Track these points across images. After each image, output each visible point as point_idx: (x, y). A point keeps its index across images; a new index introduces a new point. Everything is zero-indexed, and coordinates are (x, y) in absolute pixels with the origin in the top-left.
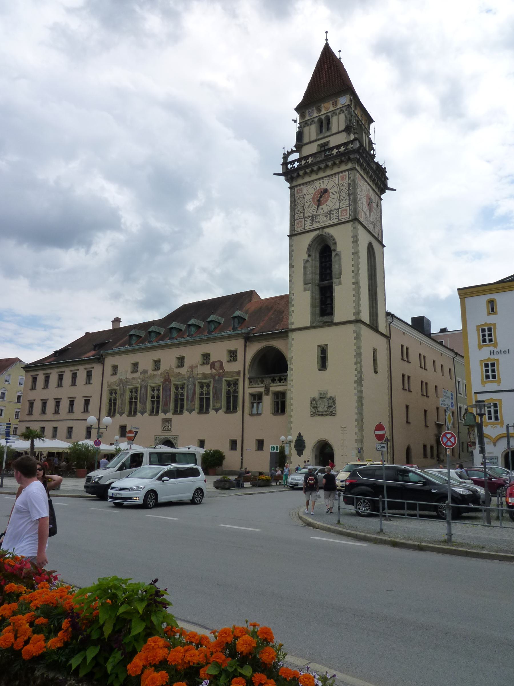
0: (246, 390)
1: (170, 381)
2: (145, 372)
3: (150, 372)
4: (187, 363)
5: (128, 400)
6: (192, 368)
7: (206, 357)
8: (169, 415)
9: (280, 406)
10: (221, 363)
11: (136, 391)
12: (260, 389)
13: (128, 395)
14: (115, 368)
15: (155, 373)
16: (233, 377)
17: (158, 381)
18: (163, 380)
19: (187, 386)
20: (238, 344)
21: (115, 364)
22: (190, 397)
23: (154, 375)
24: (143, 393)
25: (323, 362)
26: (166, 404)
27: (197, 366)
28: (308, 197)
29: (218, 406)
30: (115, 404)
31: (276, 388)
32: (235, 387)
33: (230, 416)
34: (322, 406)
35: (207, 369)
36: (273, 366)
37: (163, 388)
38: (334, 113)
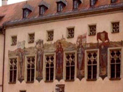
2: (40, 42)
4: (77, 33)
5: (26, 68)
6: (81, 38)
7: (93, 28)
8: (62, 82)
11: (33, 60)
13: (26, 63)
14: (14, 38)
15: (49, 43)
16: (116, 46)
17: (52, 51)
18: (56, 49)
19: (78, 54)
21: (14, 34)
22: (80, 65)
23: (48, 45)
24: (40, 62)
26: (60, 71)
27: (85, 37)
29: (104, 73)
30: (15, 72)
32: (118, 56)
33: (115, 82)
37: (57, 56)
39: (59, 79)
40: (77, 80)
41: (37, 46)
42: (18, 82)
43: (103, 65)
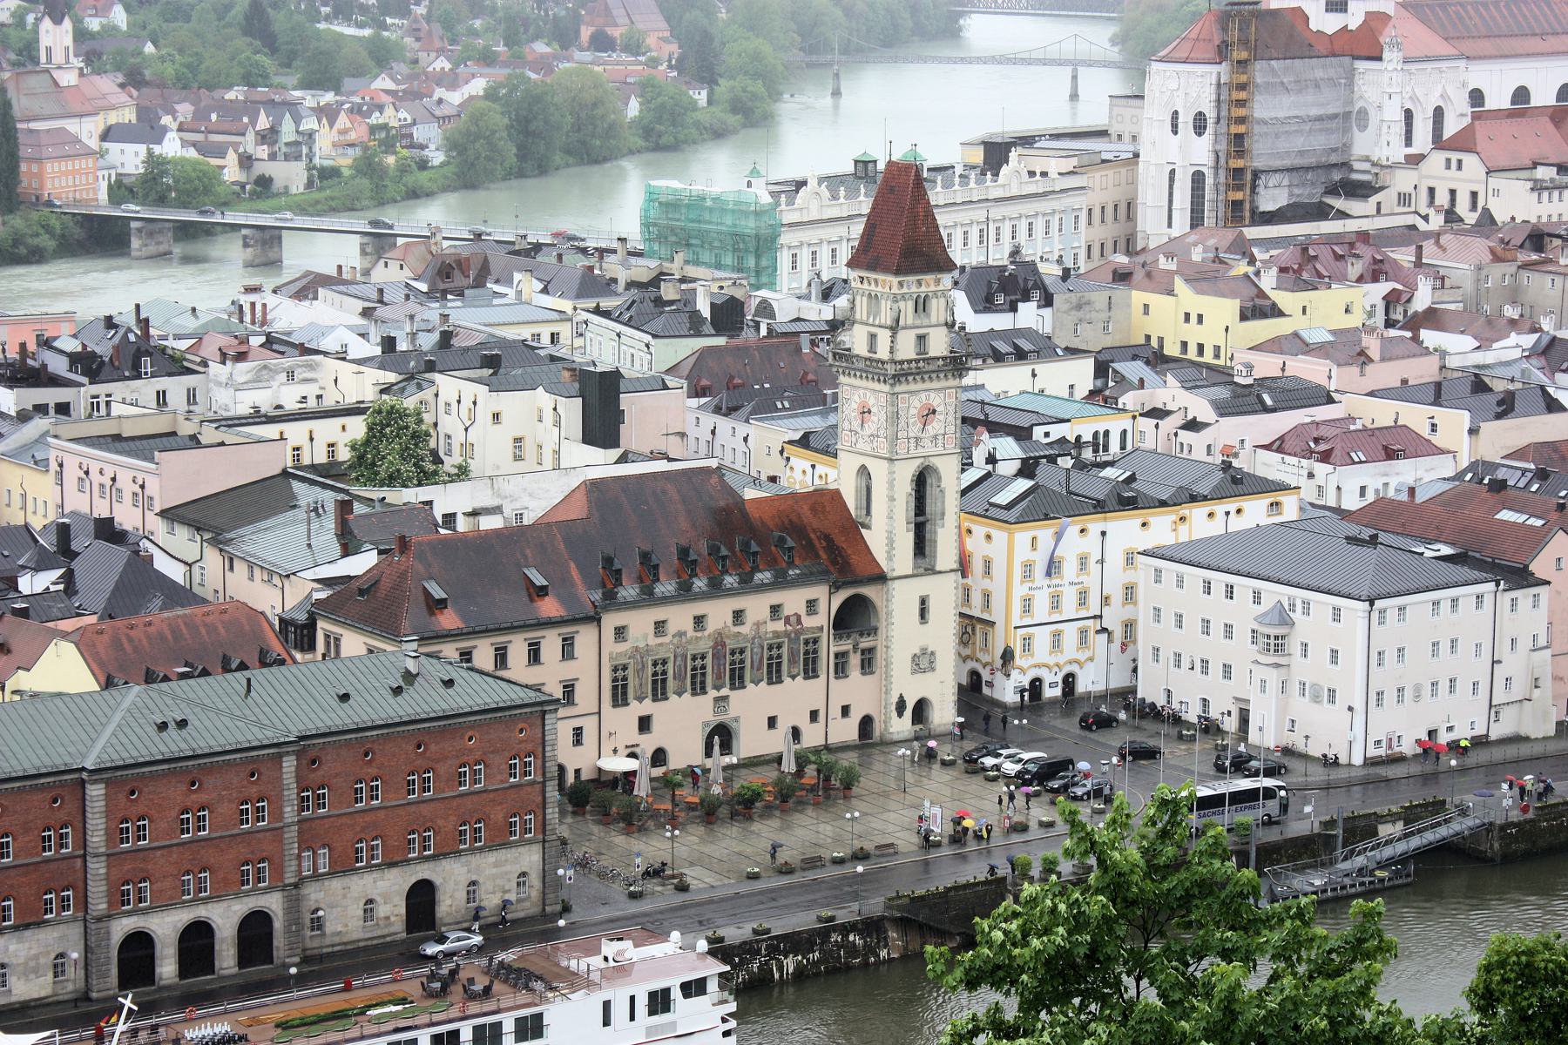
0: (829, 648)
1: (724, 645)
2: (681, 634)
3: (691, 633)
6: (758, 624)
7: (775, 610)
8: (725, 691)
9: (867, 665)
10: (799, 617)
12: (846, 646)
13: (650, 670)
15: (699, 634)
17: (705, 646)
20: (819, 592)
25: (923, 614)
28: (913, 411)
29: (795, 671)
31: (865, 643)
34: (924, 663)
35: (779, 626)
36: (854, 617)
38: (935, 293)
39: (717, 688)
40: (750, 686)
41: (675, 641)
42: (634, 704)
43: (793, 661)
